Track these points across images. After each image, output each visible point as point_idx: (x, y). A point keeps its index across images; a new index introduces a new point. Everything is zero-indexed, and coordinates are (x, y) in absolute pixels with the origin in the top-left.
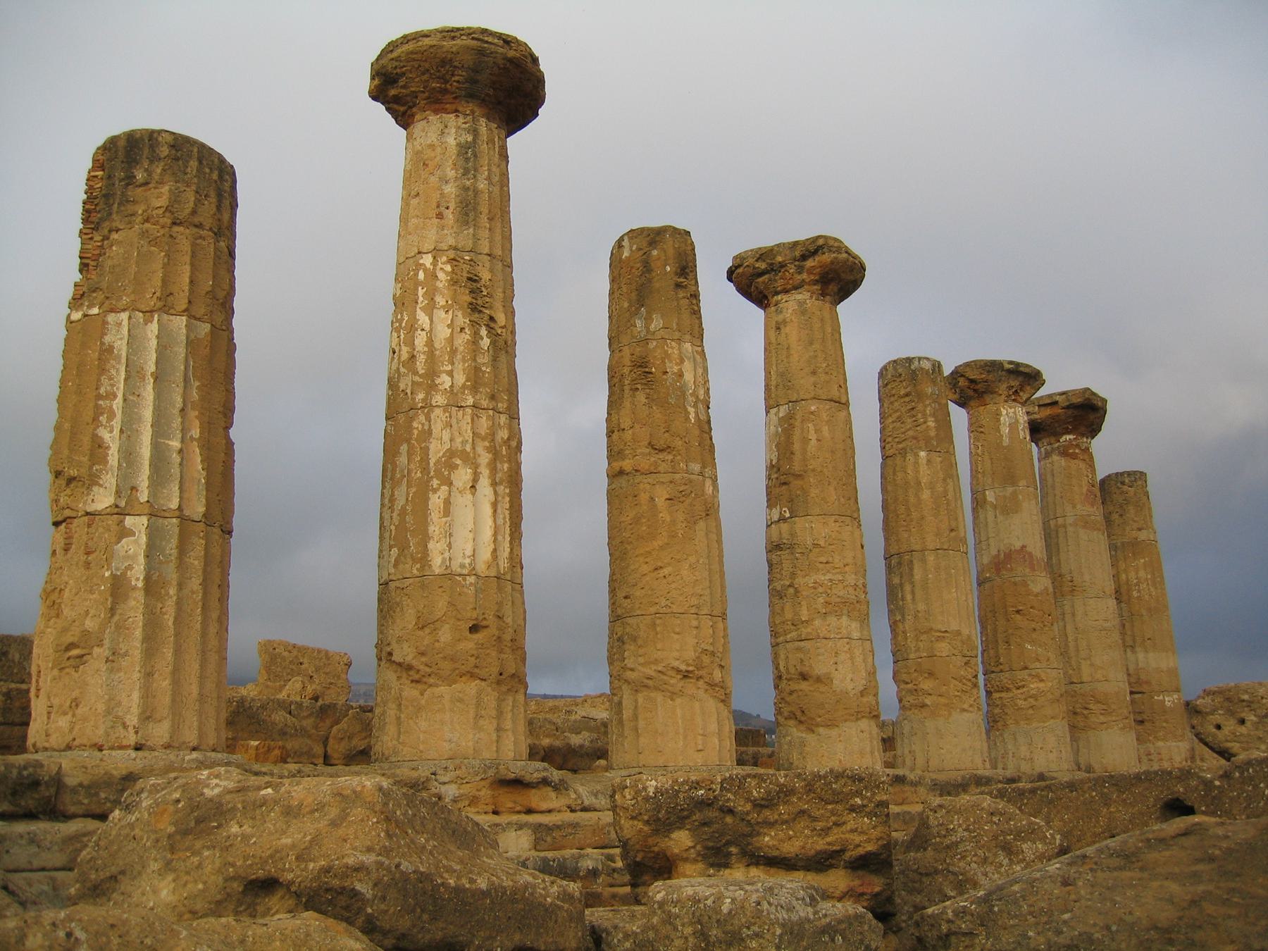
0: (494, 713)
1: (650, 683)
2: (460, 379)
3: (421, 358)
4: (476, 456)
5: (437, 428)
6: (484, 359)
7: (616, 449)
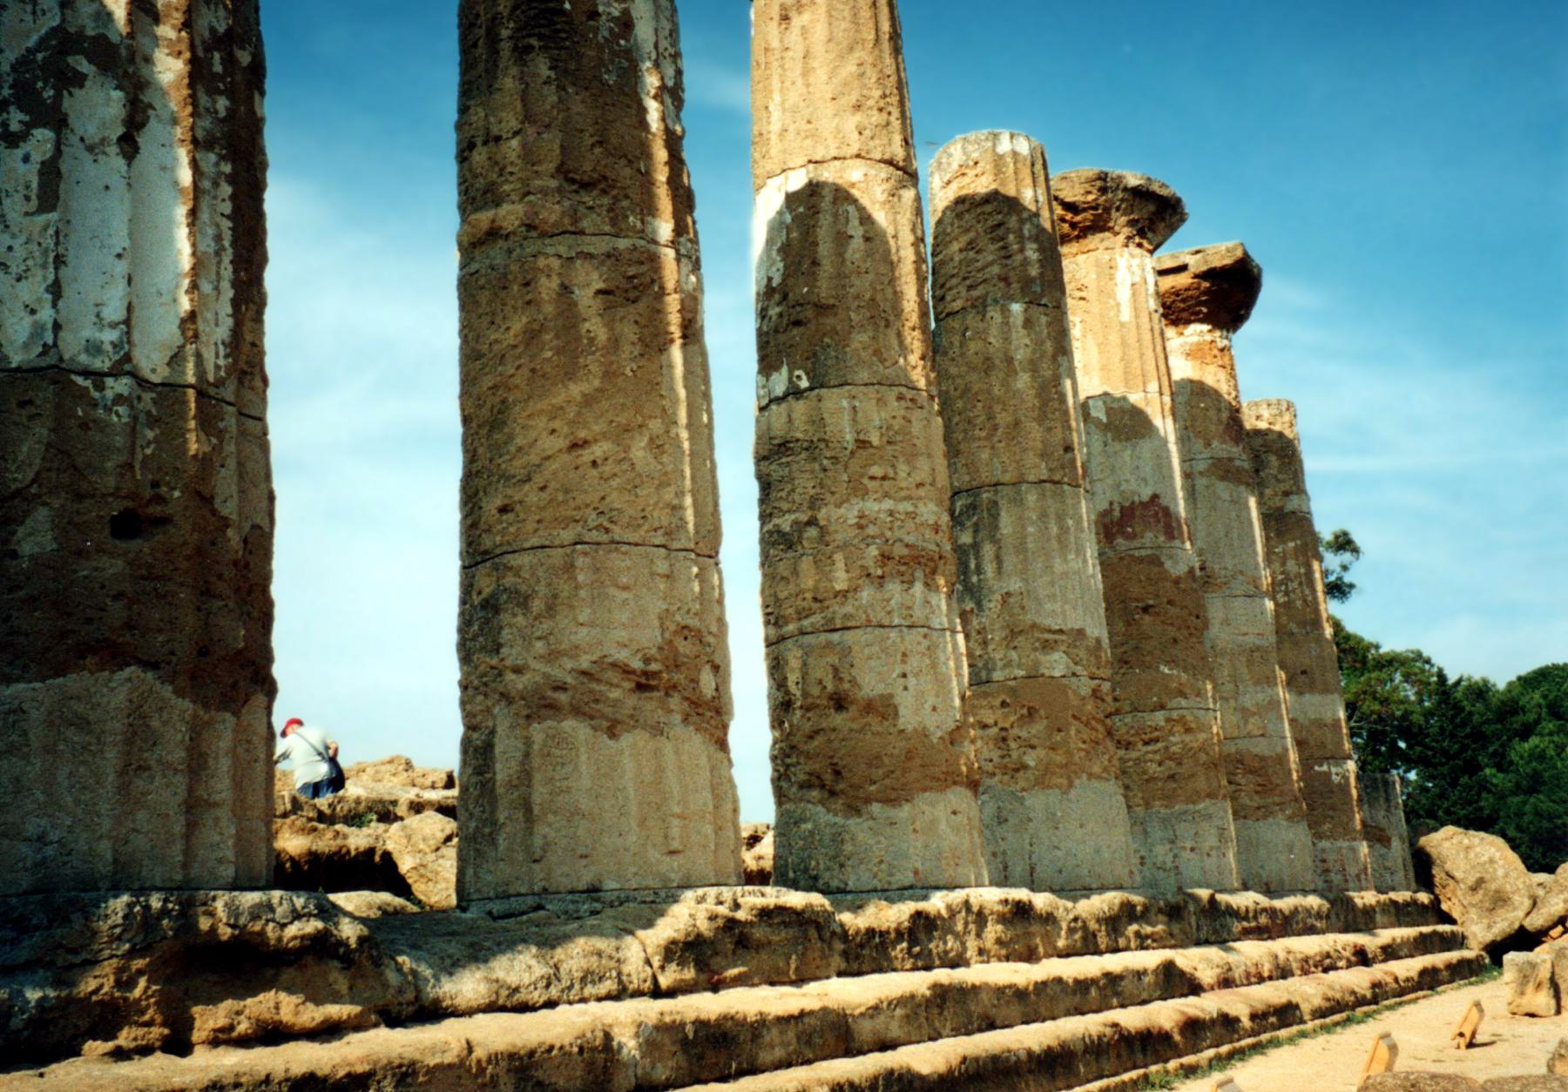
0: (179, 755)
1: (563, 697)
7: (480, 183)
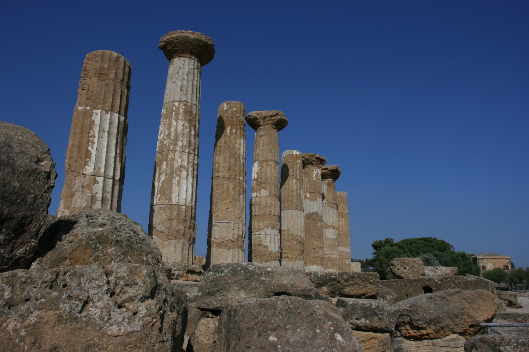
2: (185, 143)
3: (173, 135)
4: (188, 168)
5: (177, 157)
6: (192, 138)
